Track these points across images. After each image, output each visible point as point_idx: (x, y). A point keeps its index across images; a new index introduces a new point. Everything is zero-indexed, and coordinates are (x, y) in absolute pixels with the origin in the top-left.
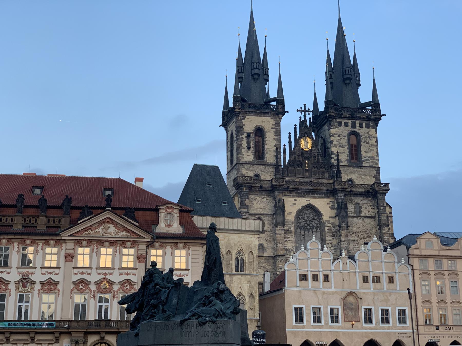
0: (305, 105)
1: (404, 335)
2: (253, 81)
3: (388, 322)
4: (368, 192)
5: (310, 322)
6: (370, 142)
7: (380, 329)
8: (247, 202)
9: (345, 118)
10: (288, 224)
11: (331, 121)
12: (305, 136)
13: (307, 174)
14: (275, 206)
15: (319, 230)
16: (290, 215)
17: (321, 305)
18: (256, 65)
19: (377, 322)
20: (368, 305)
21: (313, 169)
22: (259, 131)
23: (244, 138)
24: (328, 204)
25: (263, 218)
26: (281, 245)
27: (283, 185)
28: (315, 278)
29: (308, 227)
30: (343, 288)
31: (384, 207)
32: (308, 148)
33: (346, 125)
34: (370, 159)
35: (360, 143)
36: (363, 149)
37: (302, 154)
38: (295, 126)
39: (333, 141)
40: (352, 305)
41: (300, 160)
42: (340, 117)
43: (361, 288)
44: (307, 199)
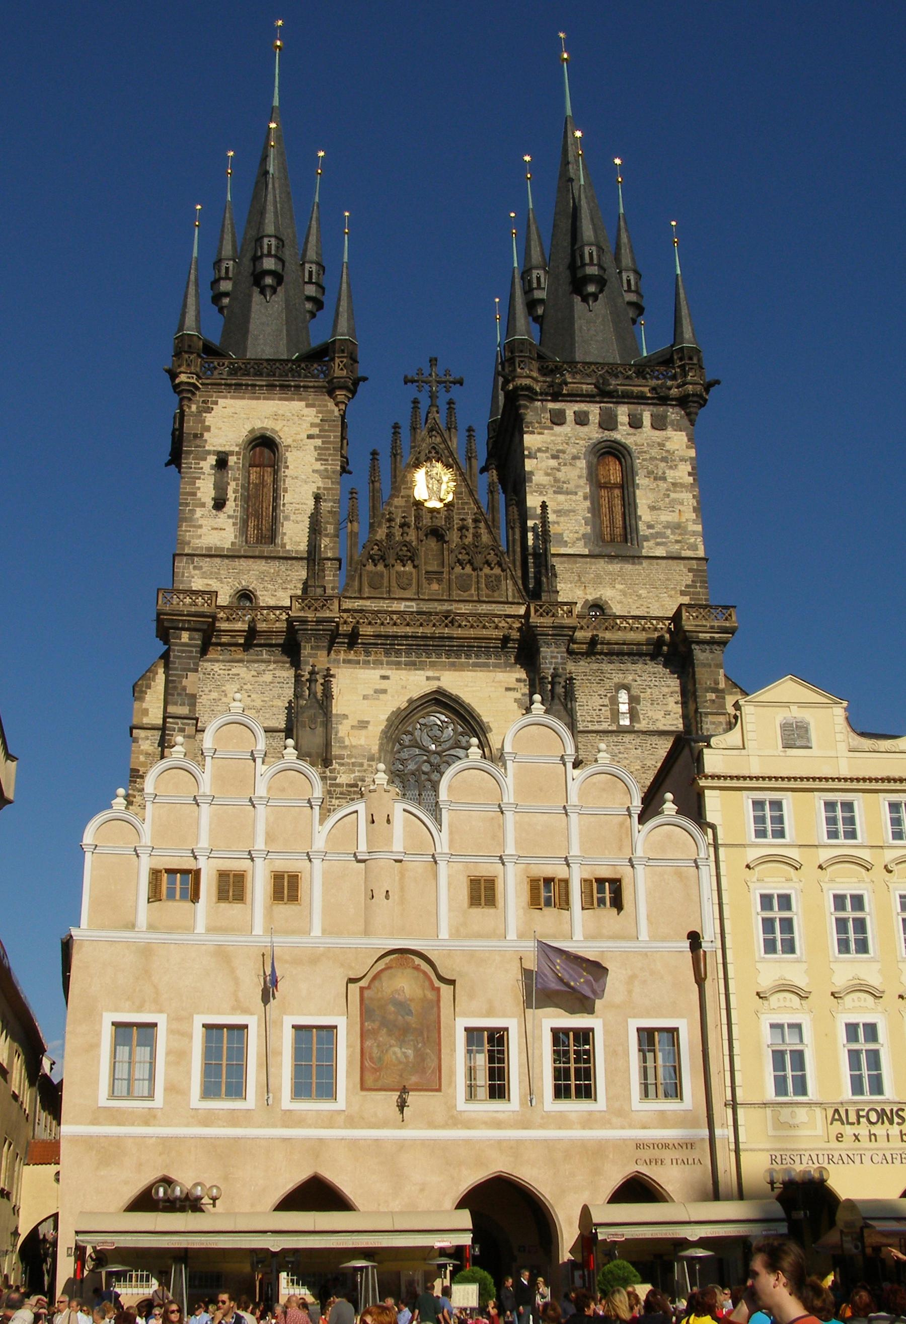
0: (433, 361)
1: (667, 1155)
2: (257, 297)
3: (586, 1092)
4: (660, 641)
5: (186, 1093)
6: (670, 474)
7: (542, 1126)
8: (190, 682)
9: (575, 397)
10: (353, 764)
11: (526, 407)
12: (428, 459)
13: (435, 586)
14: (297, 695)
16: (364, 732)
17: (246, 1011)
18: (269, 246)
19: (531, 1094)
20: (489, 1013)
21: (458, 569)
24: (508, 689)
27: (330, 620)
28: (232, 887)
30: (366, 933)
32: (441, 500)
33: (581, 420)
34: (669, 532)
35: (633, 480)
36: (643, 500)
37: (418, 518)
38: (396, 427)
39: (532, 473)
40: (410, 1013)
41: (408, 539)
42: (556, 397)
43: (456, 934)
44: (430, 673)
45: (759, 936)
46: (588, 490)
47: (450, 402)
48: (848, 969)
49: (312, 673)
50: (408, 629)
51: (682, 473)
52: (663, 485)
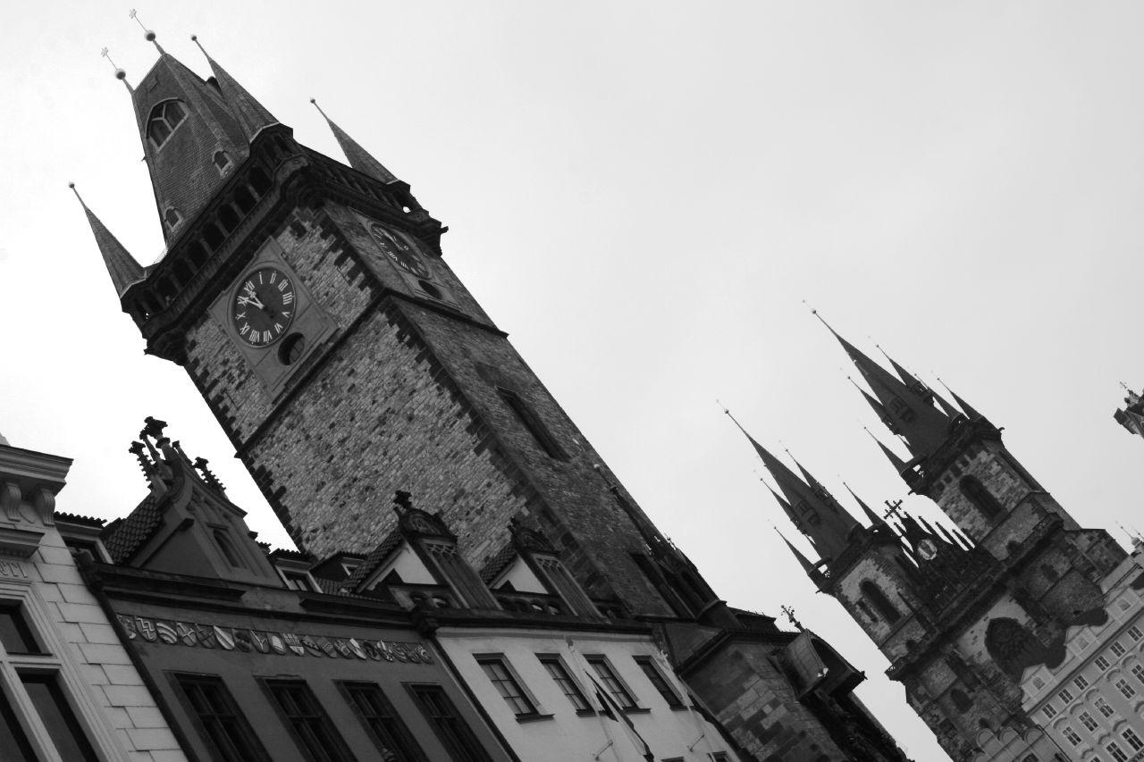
0: (887, 502)
6: (992, 472)
8: (921, 690)
9: (938, 475)
13: (959, 585)
14: (952, 669)
15: (1030, 640)
22: (868, 587)
23: (860, 612)
25: (958, 687)
26: (994, 710)
27: (939, 635)
29: (1017, 649)
31: (1072, 546)
33: (948, 480)
34: (1010, 494)
36: (992, 491)
37: (933, 566)
45: (1071, 743)
46: (973, 505)
47: (905, 513)
48: (1096, 735)
49: (950, 657)
50: (963, 612)
51: (995, 467)
52: (993, 479)
